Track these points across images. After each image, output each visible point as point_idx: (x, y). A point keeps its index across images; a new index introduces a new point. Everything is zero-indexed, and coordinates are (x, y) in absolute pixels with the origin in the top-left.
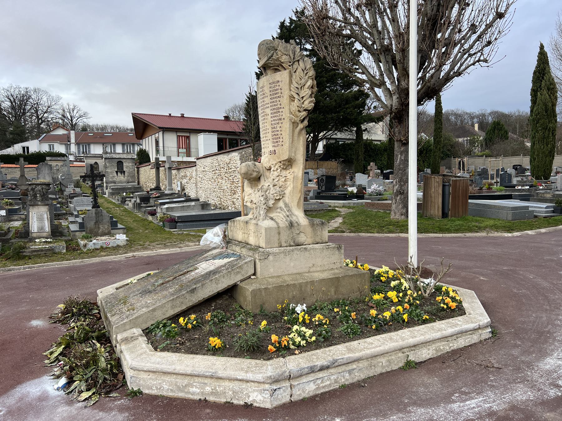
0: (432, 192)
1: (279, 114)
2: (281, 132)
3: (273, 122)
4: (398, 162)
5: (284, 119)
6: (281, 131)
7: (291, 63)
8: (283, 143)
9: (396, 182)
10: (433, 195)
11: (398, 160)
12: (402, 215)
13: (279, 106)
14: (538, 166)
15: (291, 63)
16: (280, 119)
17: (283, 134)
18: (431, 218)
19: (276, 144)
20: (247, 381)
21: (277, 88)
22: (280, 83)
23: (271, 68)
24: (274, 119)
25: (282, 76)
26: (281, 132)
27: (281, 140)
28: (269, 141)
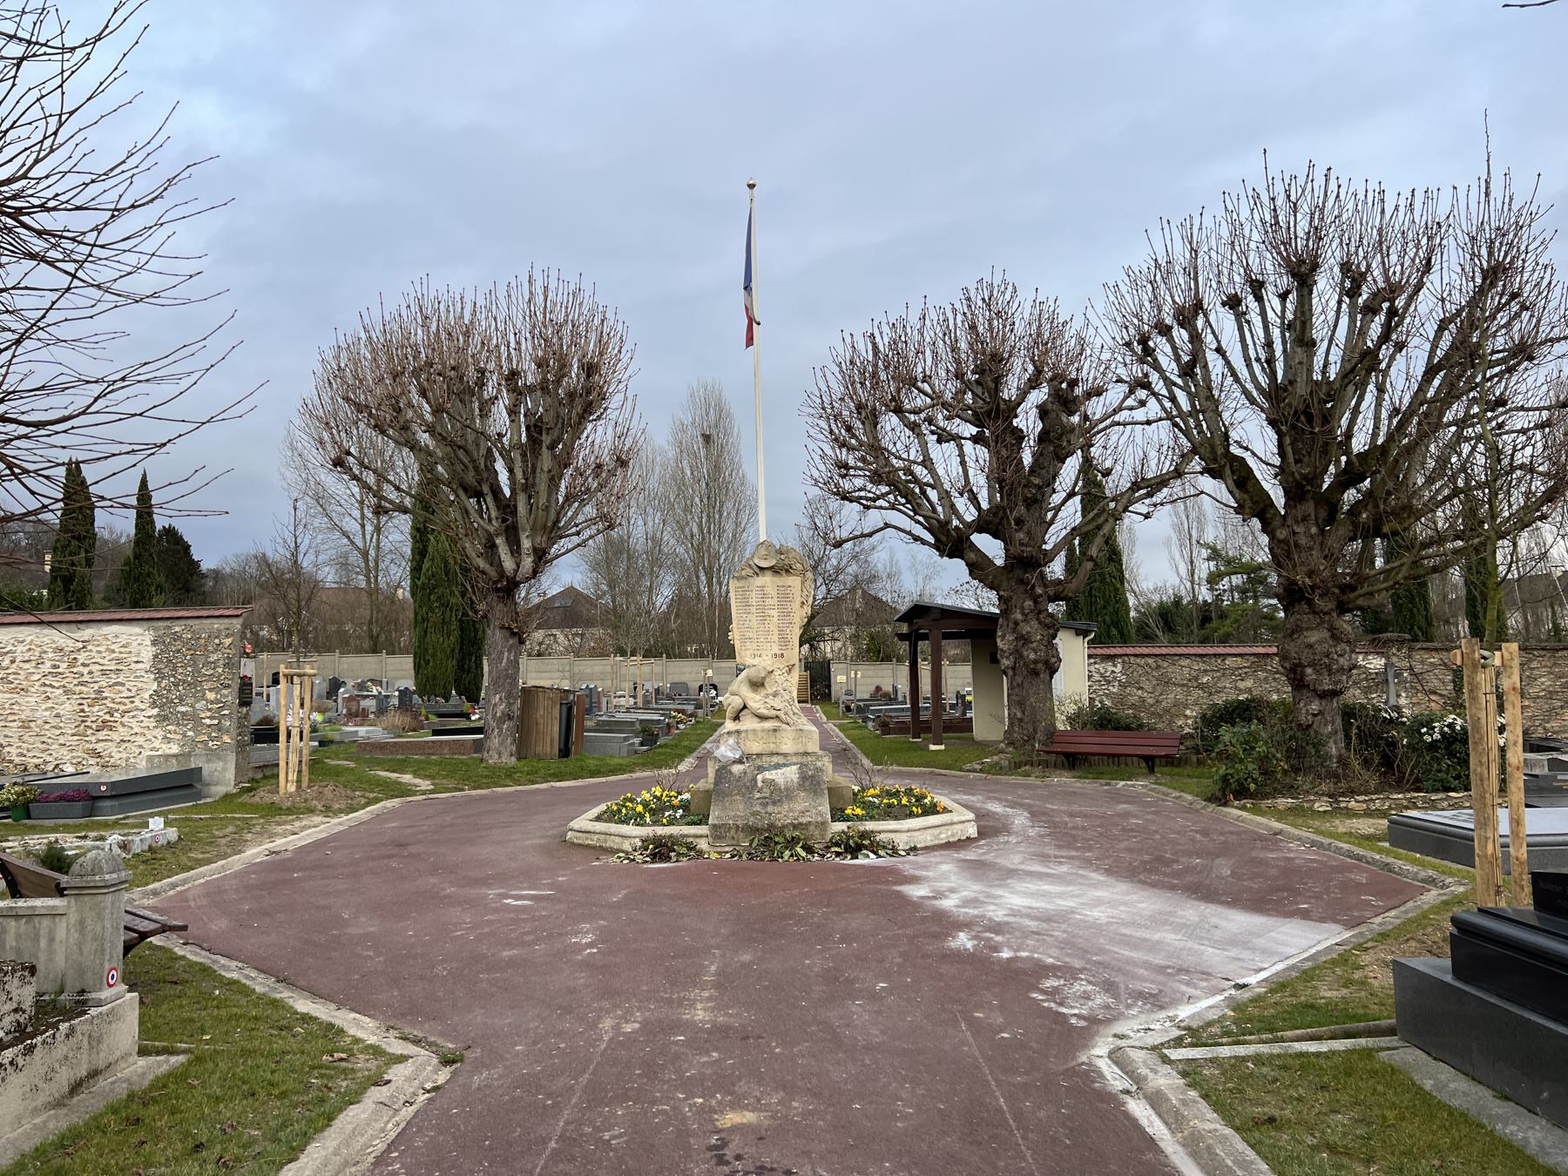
14: (434, 675)
20: (952, 824)
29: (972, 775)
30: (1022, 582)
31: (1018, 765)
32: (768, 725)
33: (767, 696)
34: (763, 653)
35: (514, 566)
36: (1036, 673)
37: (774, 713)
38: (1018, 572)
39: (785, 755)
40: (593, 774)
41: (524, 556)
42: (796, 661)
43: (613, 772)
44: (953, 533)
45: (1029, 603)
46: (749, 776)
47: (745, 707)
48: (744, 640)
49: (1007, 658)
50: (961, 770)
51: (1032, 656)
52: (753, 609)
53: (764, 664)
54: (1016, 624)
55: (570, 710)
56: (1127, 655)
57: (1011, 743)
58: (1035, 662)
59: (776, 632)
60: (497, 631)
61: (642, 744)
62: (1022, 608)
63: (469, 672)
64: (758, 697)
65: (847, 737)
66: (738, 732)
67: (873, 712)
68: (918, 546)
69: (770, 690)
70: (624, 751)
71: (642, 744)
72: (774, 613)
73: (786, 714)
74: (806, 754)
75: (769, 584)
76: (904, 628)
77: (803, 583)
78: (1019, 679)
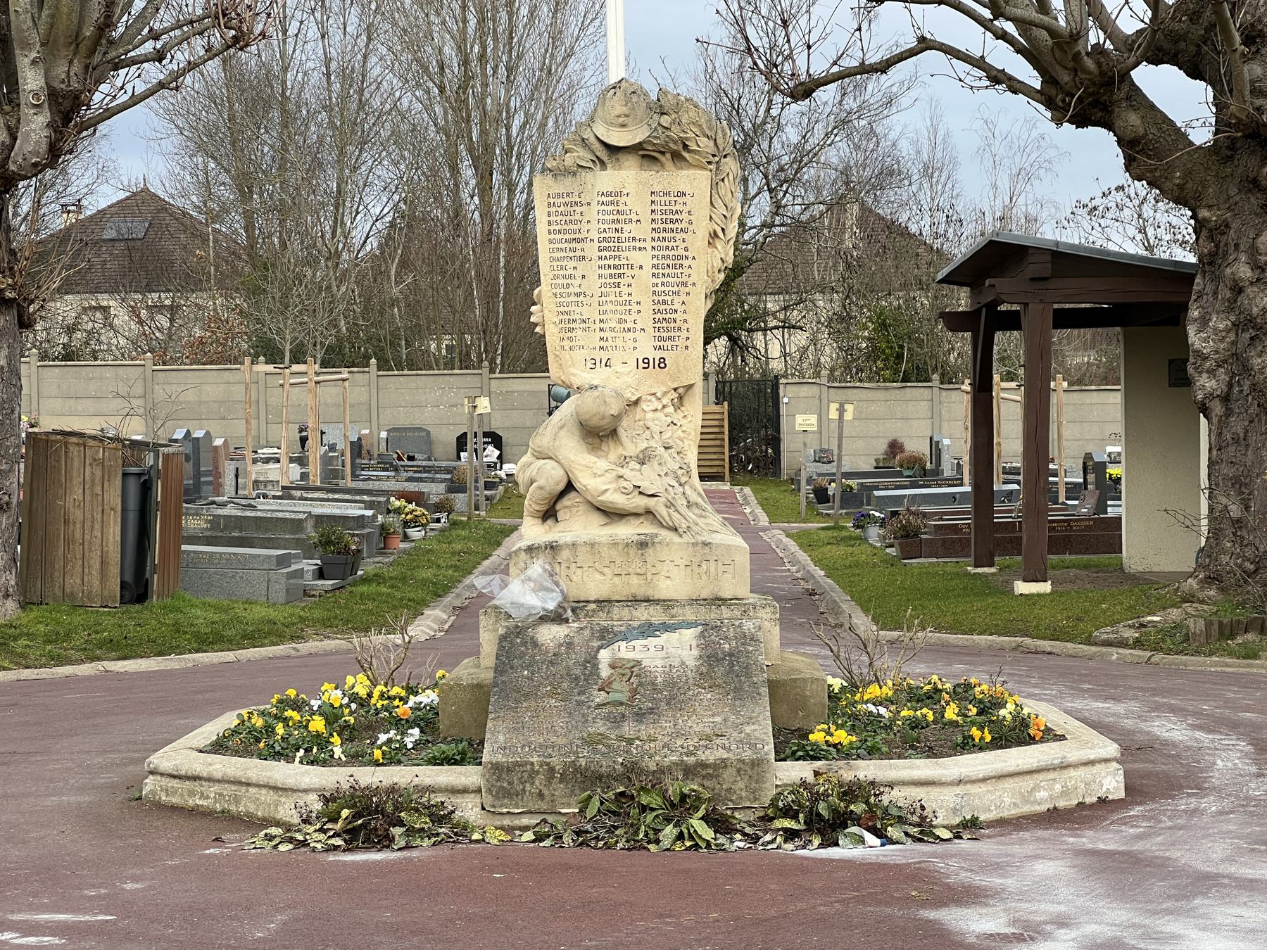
0: (70, 505)
7: (717, 159)
10: (77, 515)
15: (717, 159)
16: (685, 284)
21: (679, 207)
22: (687, 199)
23: (641, 153)
24: (665, 280)
29: (1115, 654)
32: (627, 531)
33: (624, 461)
39: (667, 604)
40: (204, 643)
46: (580, 654)
47: (570, 487)
48: (568, 322)
50: (1089, 641)
52: (592, 250)
64: (601, 464)
66: (553, 548)
72: (645, 259)
73: (670, 505)
74: (719, 601)
77: (714, 186)
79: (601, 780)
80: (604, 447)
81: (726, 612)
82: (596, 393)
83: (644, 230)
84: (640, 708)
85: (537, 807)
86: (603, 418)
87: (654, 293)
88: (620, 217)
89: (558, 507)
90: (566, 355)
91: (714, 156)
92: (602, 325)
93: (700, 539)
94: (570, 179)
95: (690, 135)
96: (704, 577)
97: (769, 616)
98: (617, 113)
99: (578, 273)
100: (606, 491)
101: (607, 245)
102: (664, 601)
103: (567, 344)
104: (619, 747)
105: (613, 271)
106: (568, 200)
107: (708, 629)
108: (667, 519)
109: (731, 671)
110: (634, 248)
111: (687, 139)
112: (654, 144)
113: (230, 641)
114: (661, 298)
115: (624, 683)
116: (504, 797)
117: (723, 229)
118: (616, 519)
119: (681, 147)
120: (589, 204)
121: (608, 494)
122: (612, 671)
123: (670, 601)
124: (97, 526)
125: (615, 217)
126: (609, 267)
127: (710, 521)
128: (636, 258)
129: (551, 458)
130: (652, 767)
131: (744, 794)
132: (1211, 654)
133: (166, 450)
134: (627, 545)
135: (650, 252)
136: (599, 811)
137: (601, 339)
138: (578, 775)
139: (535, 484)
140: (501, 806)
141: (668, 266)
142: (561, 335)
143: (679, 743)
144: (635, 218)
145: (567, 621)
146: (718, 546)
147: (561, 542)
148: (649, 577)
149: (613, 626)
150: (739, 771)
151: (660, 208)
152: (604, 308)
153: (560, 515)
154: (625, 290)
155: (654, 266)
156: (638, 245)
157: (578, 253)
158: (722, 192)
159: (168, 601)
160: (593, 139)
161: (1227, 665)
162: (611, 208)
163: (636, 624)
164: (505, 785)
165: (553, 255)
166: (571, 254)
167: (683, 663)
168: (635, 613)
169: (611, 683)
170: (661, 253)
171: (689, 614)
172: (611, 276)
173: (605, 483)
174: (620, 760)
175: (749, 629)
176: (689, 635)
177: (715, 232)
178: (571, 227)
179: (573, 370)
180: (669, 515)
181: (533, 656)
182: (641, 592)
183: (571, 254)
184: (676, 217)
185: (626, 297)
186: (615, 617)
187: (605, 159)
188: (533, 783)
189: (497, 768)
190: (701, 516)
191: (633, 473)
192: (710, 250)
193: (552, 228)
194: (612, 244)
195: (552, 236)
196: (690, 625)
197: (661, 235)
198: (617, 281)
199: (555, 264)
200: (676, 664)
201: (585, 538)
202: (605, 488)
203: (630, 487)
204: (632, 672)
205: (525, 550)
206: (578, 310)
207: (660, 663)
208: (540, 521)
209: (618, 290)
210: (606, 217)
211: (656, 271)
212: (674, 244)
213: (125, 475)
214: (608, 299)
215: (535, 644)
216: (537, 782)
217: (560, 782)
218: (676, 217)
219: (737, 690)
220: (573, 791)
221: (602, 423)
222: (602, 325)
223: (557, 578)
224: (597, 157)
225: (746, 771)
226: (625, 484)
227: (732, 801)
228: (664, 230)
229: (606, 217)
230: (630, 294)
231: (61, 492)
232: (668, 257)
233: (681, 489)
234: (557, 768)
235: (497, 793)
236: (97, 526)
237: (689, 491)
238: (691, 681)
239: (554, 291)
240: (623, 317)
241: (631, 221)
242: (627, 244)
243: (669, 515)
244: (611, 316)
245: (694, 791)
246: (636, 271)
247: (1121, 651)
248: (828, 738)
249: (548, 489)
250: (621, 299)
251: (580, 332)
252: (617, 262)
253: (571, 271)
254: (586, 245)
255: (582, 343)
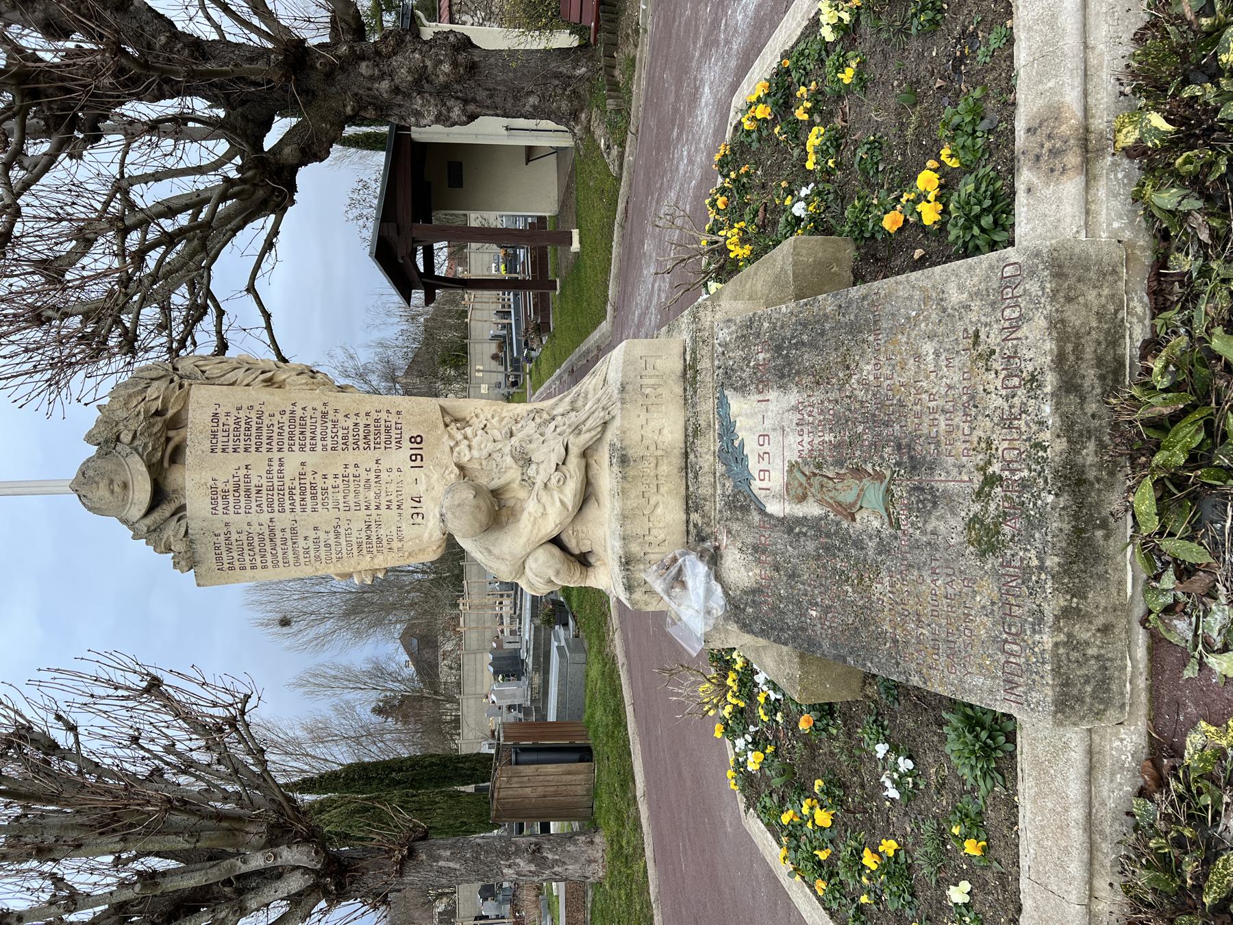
0: (534, 795)
1: (308, 419)
2: (363, 414)
3: (329, 442)
4: (457, 866)
5: (325, 404)
6: (357, 415)
7: (176, 378)
8: (393, 411)
9: (510, 866)
10: (540, 791)
11: (452, 865)
12: (592, 842)
13: (286, 417)
14: (477, 815)
15: (176, 378)
16: (325, 415)
17: (368, 409)
18: (593, 792)
19: (393, 432)
21: (231, 421)
22: (220, 411)
23: (166, 464)
24: (319, 437)
25: (203, 402)
26: (363, 414)
27: (383, 415)
28: (384, 465)
29: (629, 159)
30: (329, 76)
31: (614, 86)
32: (606, 479)
33: (527, 482)
34: (409, 490)
35: (298, 874)
36: (472, 67)
37: (574, 462)
38: (315, 81)
39: (692, 433)
40: (620, 723)
41: (279, 862)
42: (430, 405)
43: (616, 691)
44: (250, 174)
45: (364, 68)
46: (779, 540)
47: (556, 541)
48: (371, 544)
49: (449, 110)
50: (618, 179)
51: (446, 68)
52: (283, 520)
53: (439, 489)
54: (396, 90)
55: (525, 750)
56: (450, 6)
57: (574, 115)
58: (455, 64)
59: (351, 457)
60: (407, 879)
61: (566, 625)
62: (372, 78)
63: (474, 769)
64: (531, 507)
65: (551, 375)
66: (627, 562)
67: (520, 351)
68: (281, 241)
69: (513, 474)
70: (581, 657)
71: (566, 625)
72: (293, 462)
73: (577, 430)
74: (689, 374)
75: (207, 477)
76: (418, 296)
77: (210, 381)
78: (482, 95)
79: (1084, 530)
80: (511, 503)
81: (705, 364)
82: (449, 516)
83: (258, 462)
84: (898, 464)
85: (1123, 636)
86: (478, 507)
87: (334, 449)
88: (242, 488)
89: (577, 552)
90: (409, 546)
91: (172, 381)
92: (373, 507)
93: (616, 395)
94: (197, 547)
95: (141, 407)
96: (659, 390)
97: (709, 313)
98: (107, 494)
99: (312, 534)
100: (562, 502)
101: (276, 503)
102: (686, 436)
103: (396, 544)
104: (1006, 499)
105: (308, 496)
106: (223, 548)
107: (729, 380)
108: (593, 433)
109: (813, 345)
110: (280, 471)
111: (146, 412)
112: (154, 449)
113: (619, 705)
114: (341, 441)
115: (839, 486)
116: (1108, 690)
117: (263, 372)
118: (590, 489)
119: (159, 419)
120: (227, 524)
121: (566, 500)
122: (811, 500)
123: (686, 429)
124: (547, 778)
125: (243, 494)
126: (303, 500)
127: (591, 387)
128: (291, 468)
129: (524, 562)
130: (1061, 445)
131: (1106, 292)
132: (631, 92)
133: (502, 739)
134: (624, 478)
135: (286, 454)
136: (1191, 539)
137: (388, 507)
138: (1075, 568)
139: (553, 579)
140: (1122, 694)
141: (302, 433)
142: (385, 551)
143: (1000, 402)
144: (243, 472)
145: (717, 548)
146: (624, 375)
147: (621, 552)
148: (660, 453)
149: (723, 495)
150: (1069, 300)
151: (231, 443)
152: (352, 505)
153: (585, 550)
154: (330, 482)
155: (302, 449)
156: (276, 468)
157: (288, 535)
158: (216, 372)
159: (590, 734)
160: (149, 521)
161: (640, 77)
162: (231, 499)
163: (720, 468)
164: (1089, 689)
165: (292, 563)
166: (289, 543)
167: (795, 409)
168: (706, 468)
169: (840, 504)
170: (286, 441)
171: (707, 406)
172: (314, 497)
173: (553, 504)
174: (1050, 498)
175: (731, 334)
176: (737, 405)
177: (265, 381)
178: (256, 543)
179: (426, 536)
180: (589, 431)
181: (780, 598)
182: (677, 461)
183: (289, 543)
184: (243, 424)
185: (339, 481)
186: (710, 491)
187: (173, 506)
188: (1087, 643)
189: (1063, 703)
190: (586, 397)
191: (541, 471)
192: (288, 387)
193: (259, 565)
194: (276, 497)
195: (269, 564)
196: (723, 403)
197: (265, 441)
198: (319, 491)
199: (302, 560)
200: (796, 417)
201: (615, 525)
202: (558, 504)
203: (558, 475)
204: (815, 475)
205: (631, 593)
206: (355, 534)
207: (793, 439)
208: (589, 569)
209: (330, 490)
210: (243, 504)
211: (308, 446)
212: (276, 426)
213: (517, 763)
214: (342, 500)
215: (756, 591)
216: (1086, 636)
217: (1086, 598)
218: (243, 424)
219: (854, 329)
220: (1100, 577)
221: (484, 508)
222: (373, 507)
223: (667, 561)
224: (173, 515)
225: (1069, 288)
226: (554, 481)
227: (1116, 312)
228: (259, 437)
229: (243, 504)
230: (336, 476)
231: (527, 801)
232: (291, 433)
233: (559, 418)
234: (1063, 603)
235: (1102, 701)
236: (547, 778)
237: (559, 410)
238: (832, 396)
239: (334, 560)
240: (362, 483)
241: (247, 476)
242: (275, 480)
243: (589, 431)
244: (361, 497)
245: (1166, 367)
246: (308, 469)
247: (626, 154)
248: (931, 197)
249: (558, 566)
250: (341, 486)
251: (382, 532)
252: (297, 491)
253: (310, 543)
254: (278, 526)
255: (394, 529)
